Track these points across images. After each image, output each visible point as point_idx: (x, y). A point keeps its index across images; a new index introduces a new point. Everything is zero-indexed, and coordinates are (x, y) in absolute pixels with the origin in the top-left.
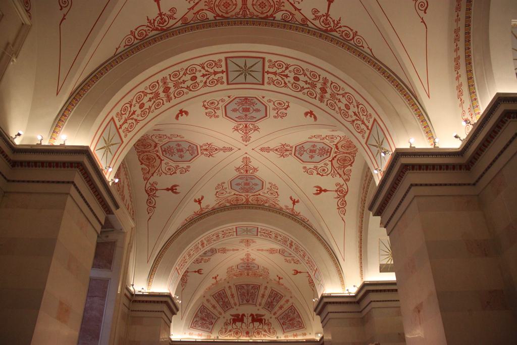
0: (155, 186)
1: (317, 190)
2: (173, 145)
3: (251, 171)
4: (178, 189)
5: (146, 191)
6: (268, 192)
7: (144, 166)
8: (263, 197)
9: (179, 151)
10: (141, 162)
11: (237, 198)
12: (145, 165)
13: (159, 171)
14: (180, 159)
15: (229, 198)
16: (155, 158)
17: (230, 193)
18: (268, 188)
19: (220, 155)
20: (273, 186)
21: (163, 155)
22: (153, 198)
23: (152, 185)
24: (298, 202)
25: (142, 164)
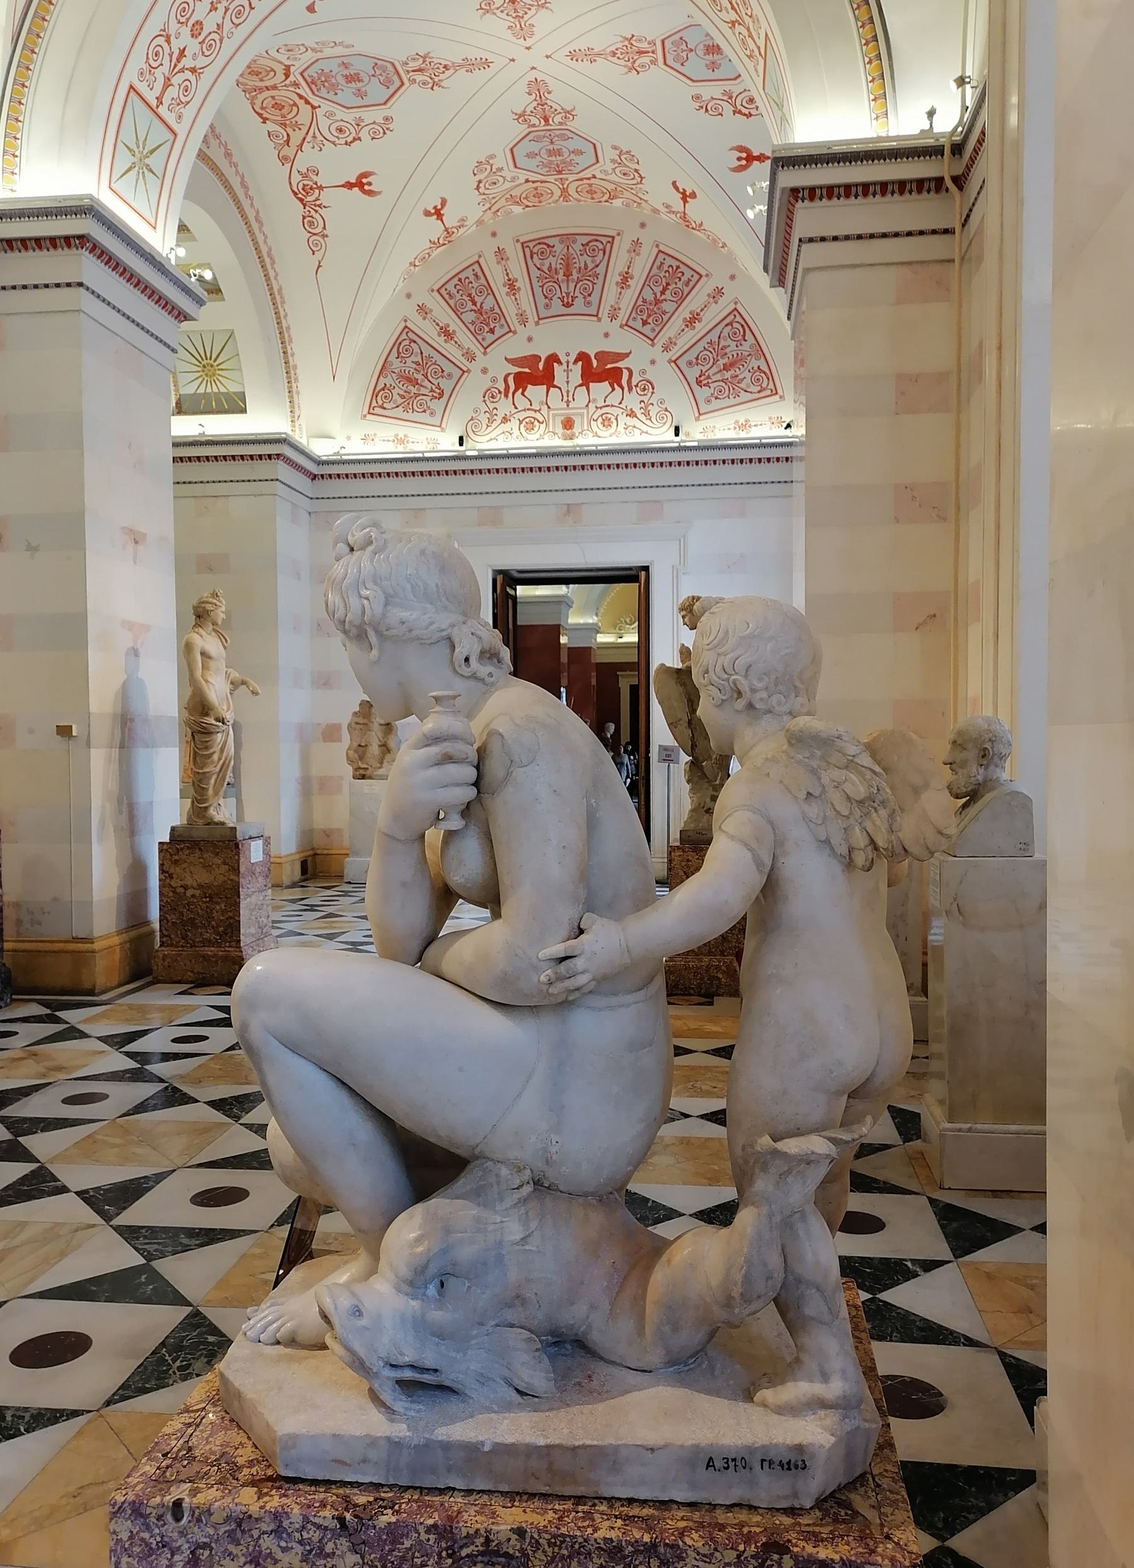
0: (315, 178)
1: (739, 159)
2: (332, 66)
3: (558, 119)
4: (376, 184)
5: (295, 194)
6: (614, 169)
7: (271, 126)
8: (603, 183)
9: (352, 78)
10: (260, 115)
11: (536, 189)
12: (274, 122)
13: (314, 137)
14: (359, 101)
15: (516, 192)
16: (295, 104)
17: (513, 179)
18: (613, 161)
19: (458, 81)
20: (623, 156)
21: (313, 93)
22: (316, 211)
23: (305, 176)
24: (693, 195)
25: (265, 120)
